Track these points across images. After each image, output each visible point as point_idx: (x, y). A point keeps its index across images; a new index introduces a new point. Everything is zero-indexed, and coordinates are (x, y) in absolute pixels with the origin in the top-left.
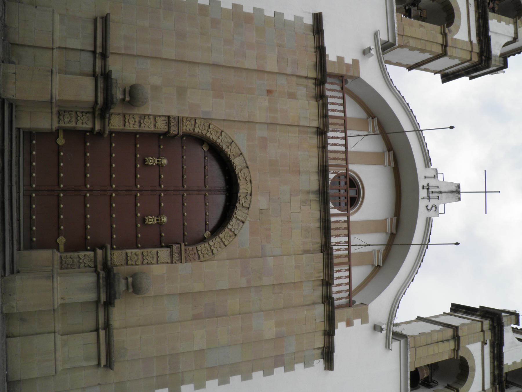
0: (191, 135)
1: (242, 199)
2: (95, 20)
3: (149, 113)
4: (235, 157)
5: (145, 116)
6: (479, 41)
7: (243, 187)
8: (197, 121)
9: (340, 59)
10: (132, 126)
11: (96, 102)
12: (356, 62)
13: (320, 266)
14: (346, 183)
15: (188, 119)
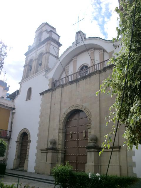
0: (65, 125)
1: (76, 108)
2: (42, 153)
3: (58, 138)
4: (67, 112)
5: (59, 139)
6: (45, 42)
7: (74, 108)
8: (60, 124)
9: (49, 85)
10: (60, 142)
11: (52, 152)
12: (49, 80)
13: (95, 76)
14: (82, 71)
15: (59, 127)
